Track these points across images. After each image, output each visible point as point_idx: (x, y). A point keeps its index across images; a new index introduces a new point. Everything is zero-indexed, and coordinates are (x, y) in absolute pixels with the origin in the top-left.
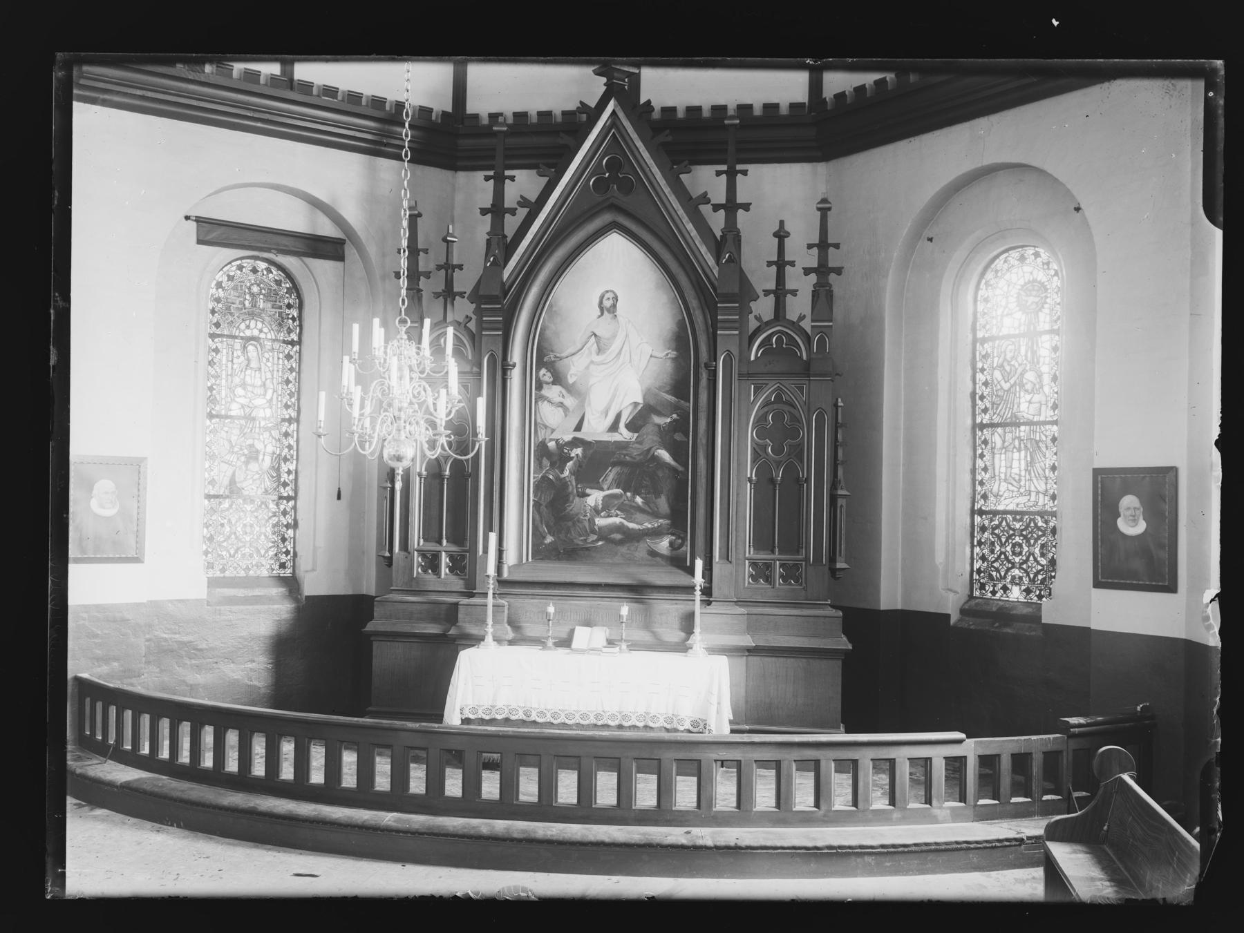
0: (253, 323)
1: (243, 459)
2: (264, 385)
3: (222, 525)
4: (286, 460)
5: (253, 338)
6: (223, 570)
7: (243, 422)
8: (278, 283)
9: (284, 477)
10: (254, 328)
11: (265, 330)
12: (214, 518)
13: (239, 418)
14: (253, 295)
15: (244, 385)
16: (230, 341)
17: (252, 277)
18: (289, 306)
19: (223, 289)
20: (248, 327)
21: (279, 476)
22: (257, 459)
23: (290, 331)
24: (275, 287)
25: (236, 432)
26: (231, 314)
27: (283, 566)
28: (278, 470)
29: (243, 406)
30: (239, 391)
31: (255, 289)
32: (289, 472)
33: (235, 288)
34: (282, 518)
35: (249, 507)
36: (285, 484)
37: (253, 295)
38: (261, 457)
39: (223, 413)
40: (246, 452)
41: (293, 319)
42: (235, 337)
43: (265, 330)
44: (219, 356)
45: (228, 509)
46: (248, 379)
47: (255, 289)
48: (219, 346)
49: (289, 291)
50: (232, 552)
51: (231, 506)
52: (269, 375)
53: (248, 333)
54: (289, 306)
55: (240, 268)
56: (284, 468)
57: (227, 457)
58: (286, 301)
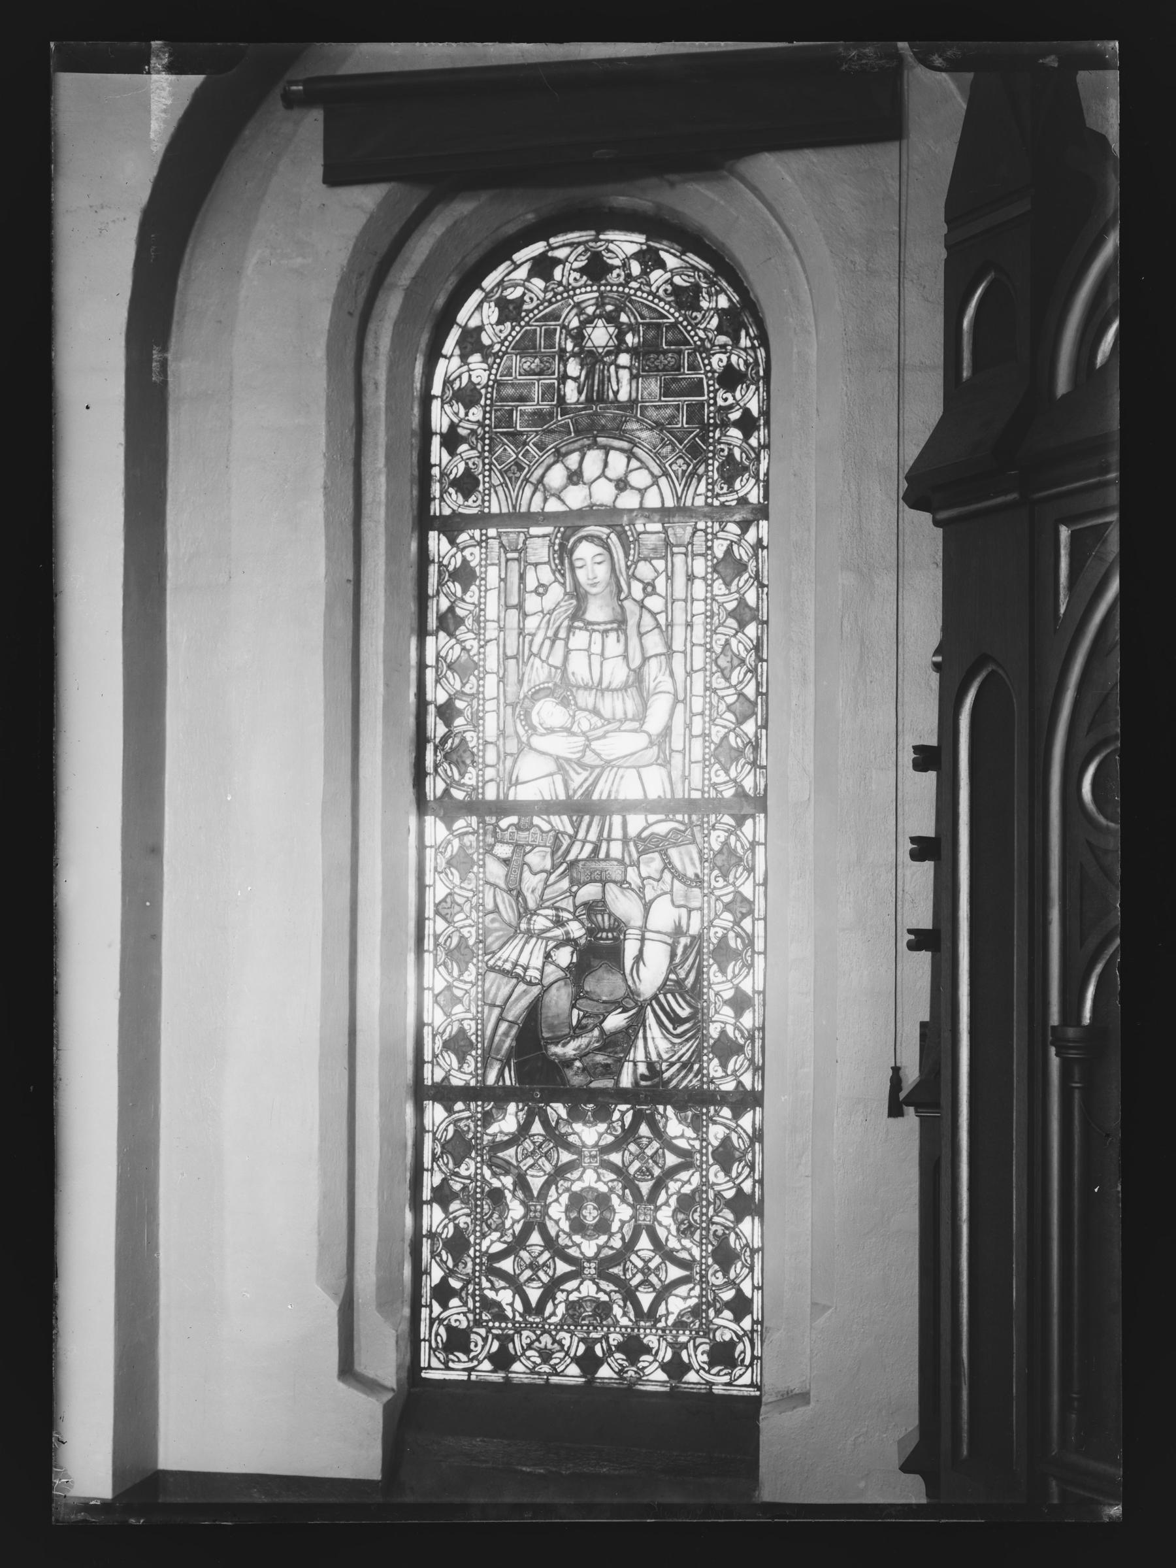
0: (593, 459)
1: (564, 956)
2: (638, 676)
3: (497, 1196)
4: (723, 953)
5: (592, 513)
6: (502, 1360)
7: (562, 823)
8: (686, 298)
9: (721, 1022)
10: (601, 477)
11: (640, 478)
12: (468, 1168)
13: (549, 808)
14: (591, 359)
15: (562, 689)
16: (513, 535)
17: (588, 296)
18: (730, 378)
19: (486, 352)
20: (575, 477)
21: (699, 1020)
22: (614, 955)
23: (732, 471)
24: (673, 315)
25: (538, 859)
26: (514, 436)
27: (723, 1355)
28: (694, 993)
29: (562, 766)
30: (548, 712)
31: (600, 336)
32: (740, 1003)
33: (525, 347)
34: (716, 1175)
35: (588, 1134)
36: (726, 1049)
37: (591, 359)
38: (630, 949)
39: (491, 794)
40: (576, 930)
41: (747, 424)
42: (530, 519)
43: (640, 478)
44: (473, 595)
45: (514, 1140)
46: (578, 667)
47: (600, 336)
48: (474, 556)
49: (731, 323)
50: (534, 1295)
51: (524, 1129)
52: (654, 643)
53: (576, 498)
54: (730, 378)
55: (543, 267)
56: (720, 984)
57: (510, 953)
58: (718, 361)
